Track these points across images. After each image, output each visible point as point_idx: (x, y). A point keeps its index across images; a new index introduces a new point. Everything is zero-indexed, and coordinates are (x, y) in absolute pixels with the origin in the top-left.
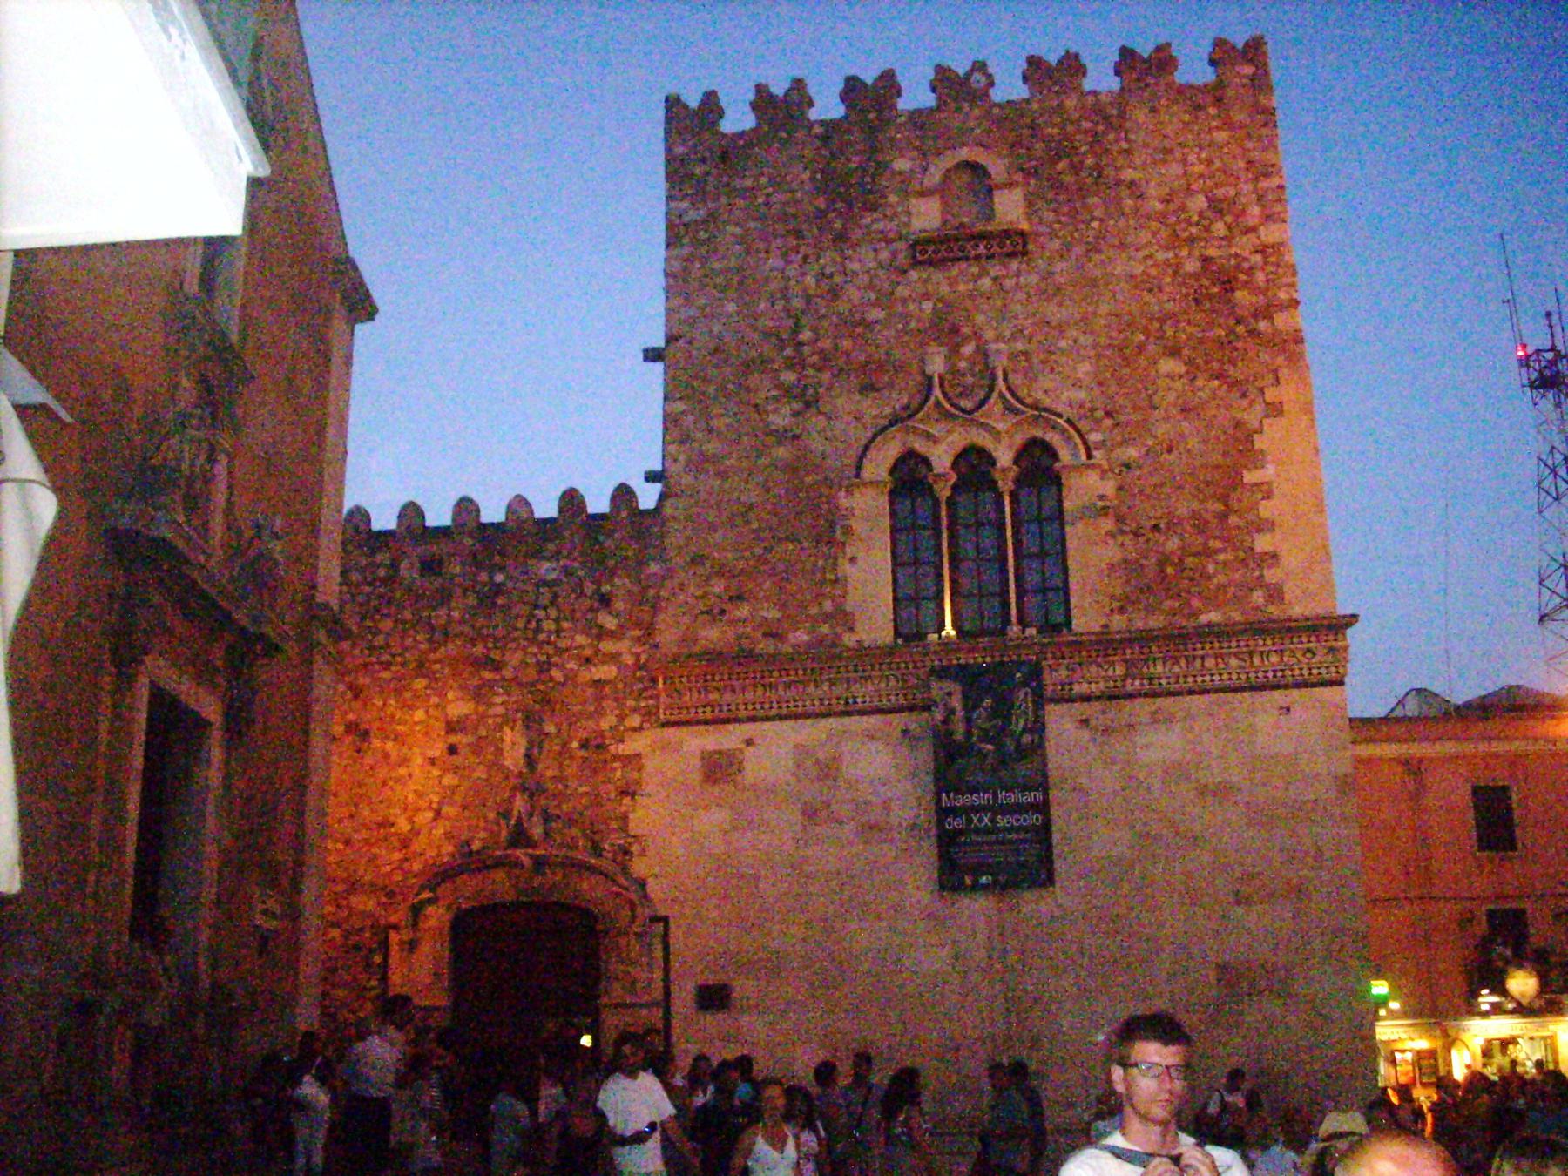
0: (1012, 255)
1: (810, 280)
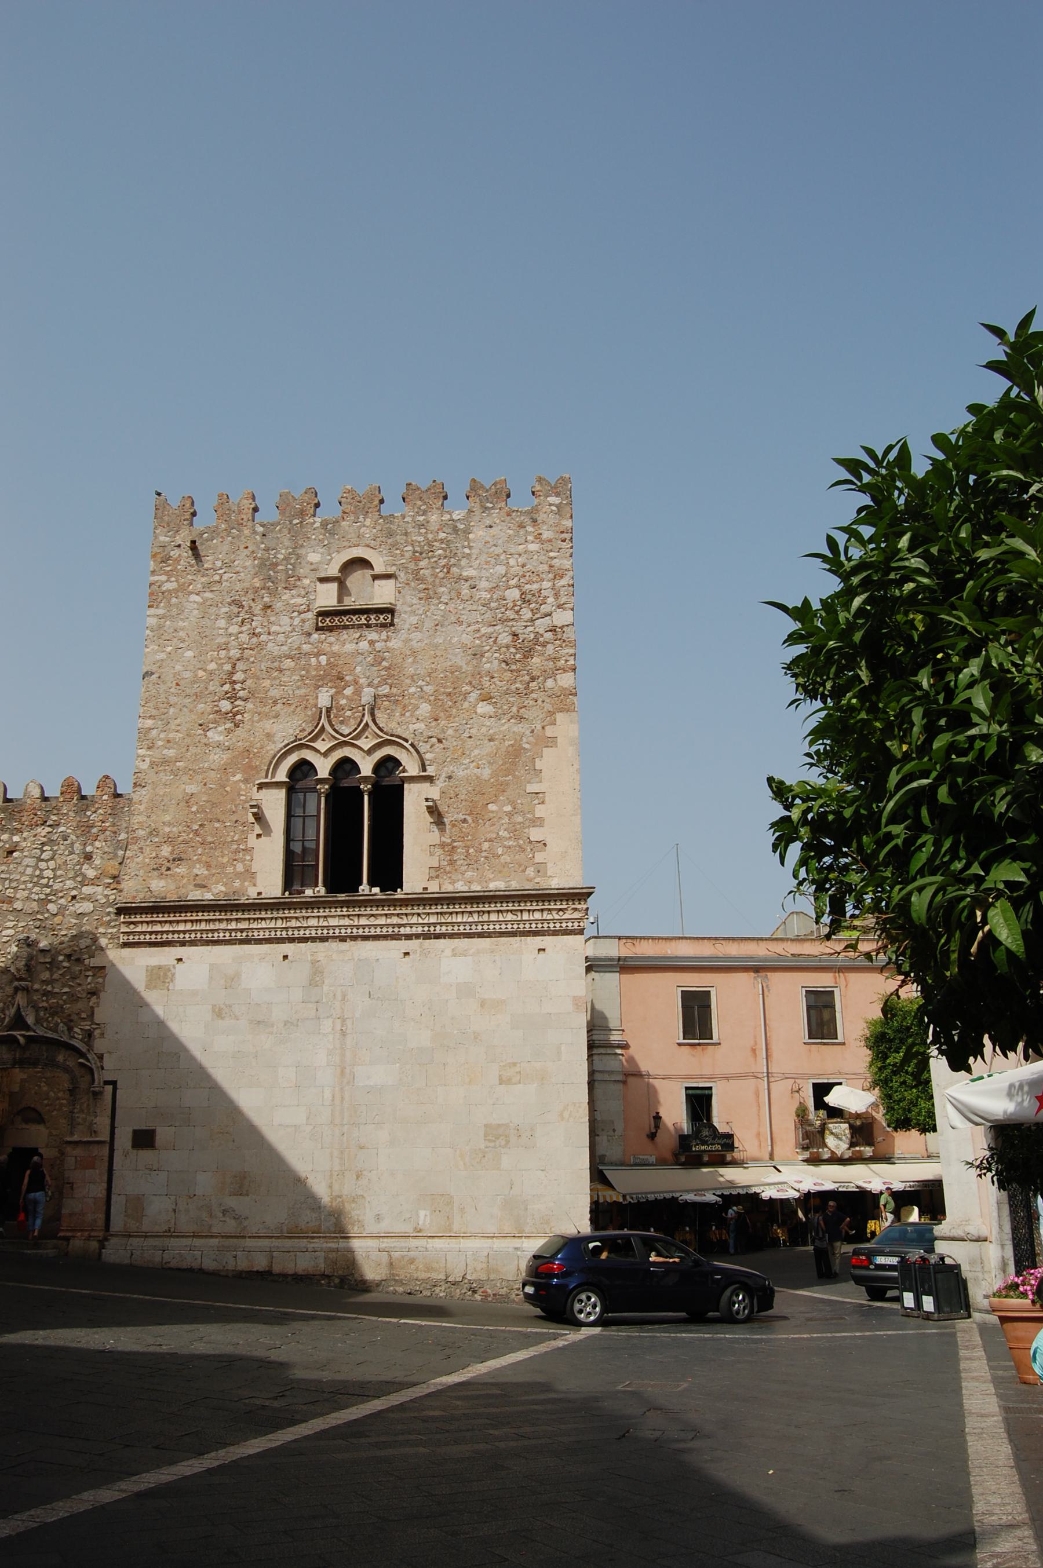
0: (384, 626)
1: (244, 637)
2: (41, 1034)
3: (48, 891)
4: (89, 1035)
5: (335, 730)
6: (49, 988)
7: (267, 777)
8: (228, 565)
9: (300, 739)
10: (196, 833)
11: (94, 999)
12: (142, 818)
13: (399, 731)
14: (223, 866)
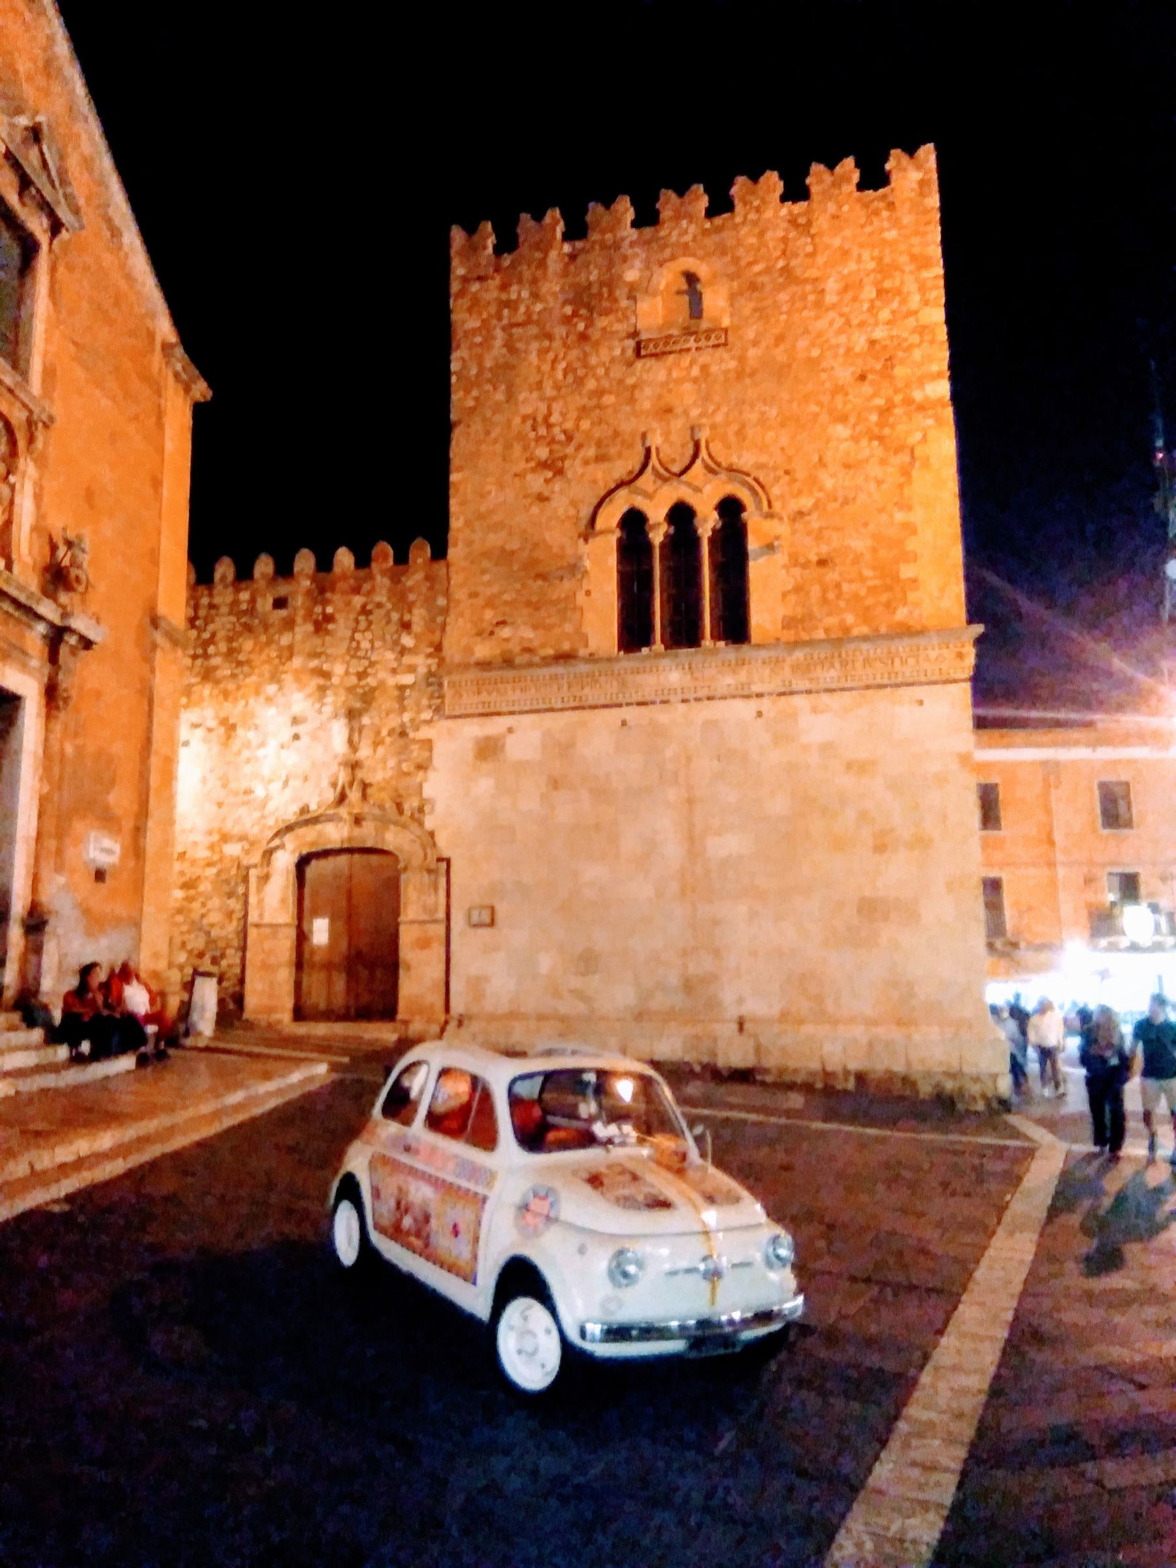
3: (366, 663)
8: (536, 296)
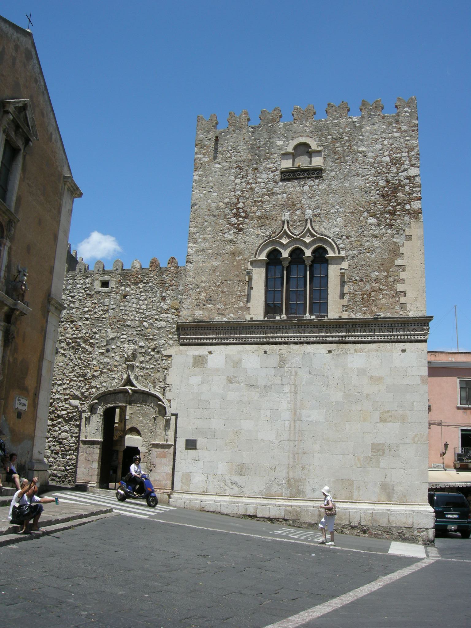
0: (317, 178)
2: (140, 388)
3: (144, 316)
4: (164, 389)
5: (291, 232)
6: (144, 365)
7: (255, 257)
9: (273, 237)
10: (219, 287)
11: (166, 372)
12: (190, 279)
13: (326, 233)
14: (233, 304)
